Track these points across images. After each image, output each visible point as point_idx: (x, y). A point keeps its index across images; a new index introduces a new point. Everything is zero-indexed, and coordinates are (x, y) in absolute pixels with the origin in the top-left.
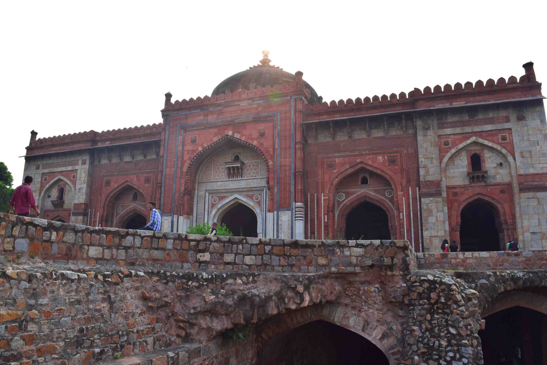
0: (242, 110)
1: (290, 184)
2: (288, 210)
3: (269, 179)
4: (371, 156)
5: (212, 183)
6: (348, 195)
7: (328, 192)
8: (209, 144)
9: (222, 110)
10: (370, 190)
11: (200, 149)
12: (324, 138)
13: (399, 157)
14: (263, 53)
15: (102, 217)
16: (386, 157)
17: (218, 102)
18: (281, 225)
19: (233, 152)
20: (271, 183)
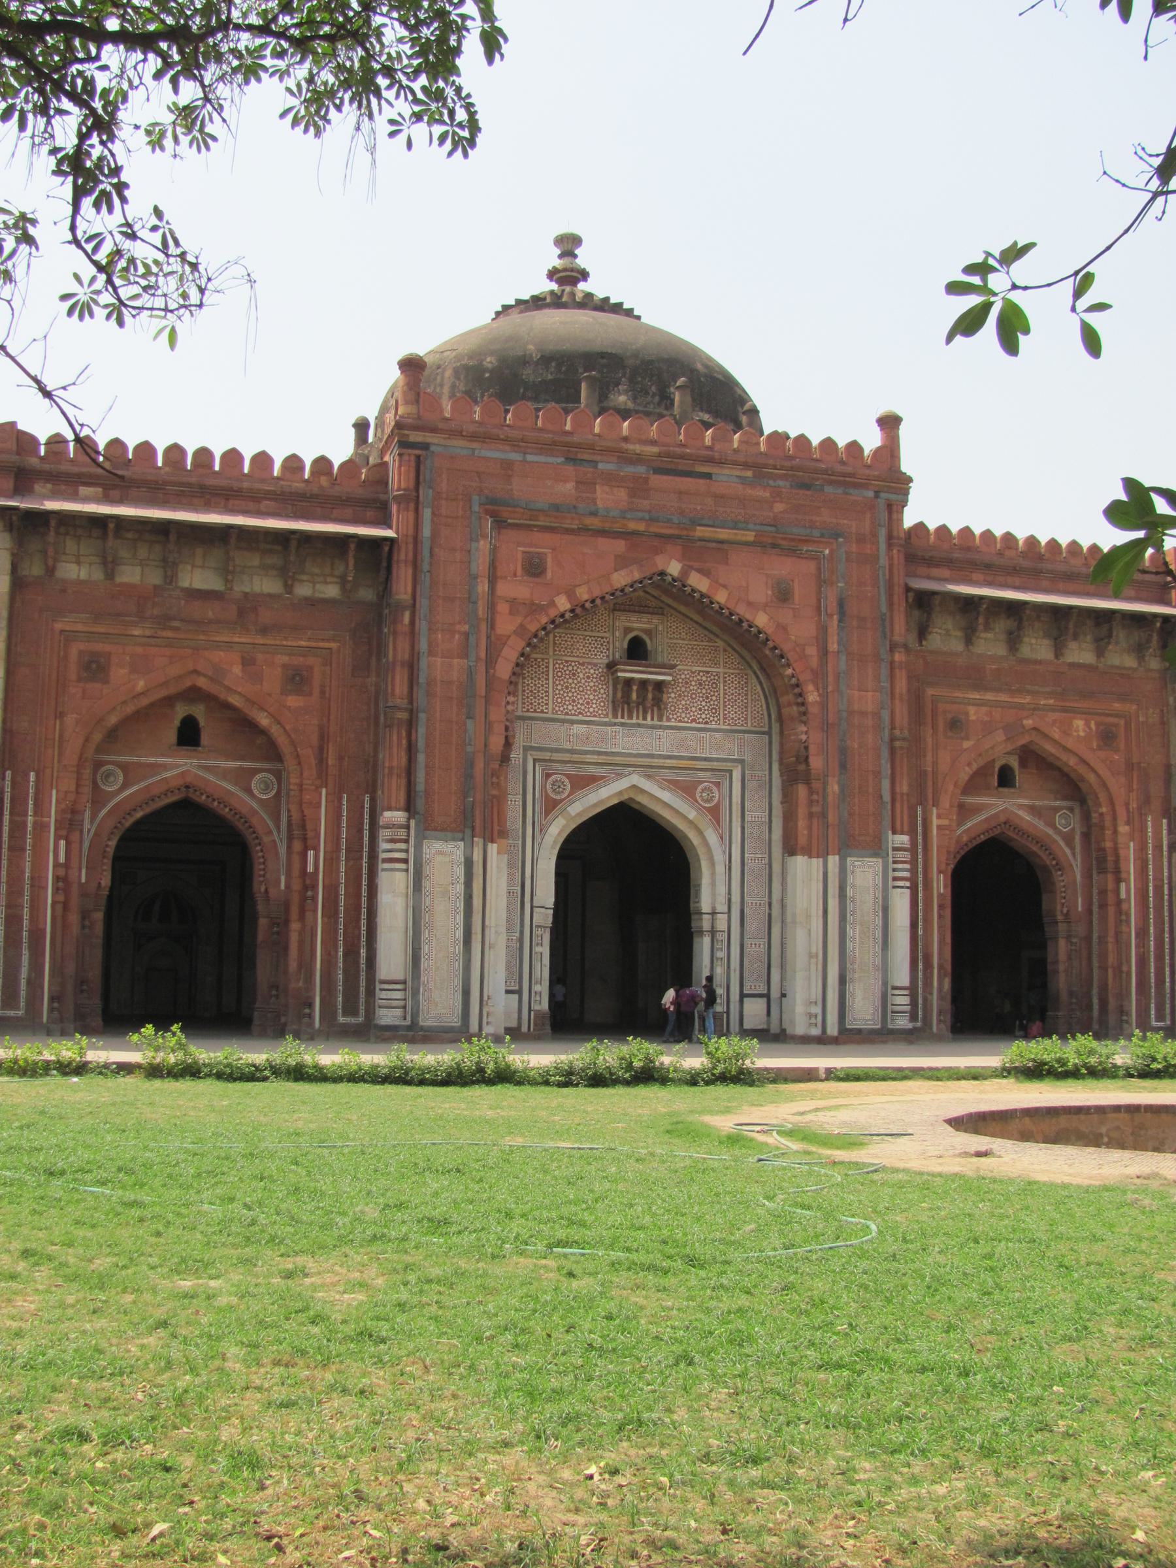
0: (719, 498)
1: (877, 774)
2: (875, 855)
3: (806, 748)
4: (1057, 715)
5: (551, 726)
6: (964, 811)
7: (947, 806)
8: (597, 592)
9: (646, 480)
10: (1021, 806)
11: (563, 603)
12: (945, 637)
13: (1122, 729)
14: (560, 241)
15: (74, 812)
16: (1093, 726)
17: (638, 448)
18: (853, 900)
19: (648, 631)
20: (816, 763)
